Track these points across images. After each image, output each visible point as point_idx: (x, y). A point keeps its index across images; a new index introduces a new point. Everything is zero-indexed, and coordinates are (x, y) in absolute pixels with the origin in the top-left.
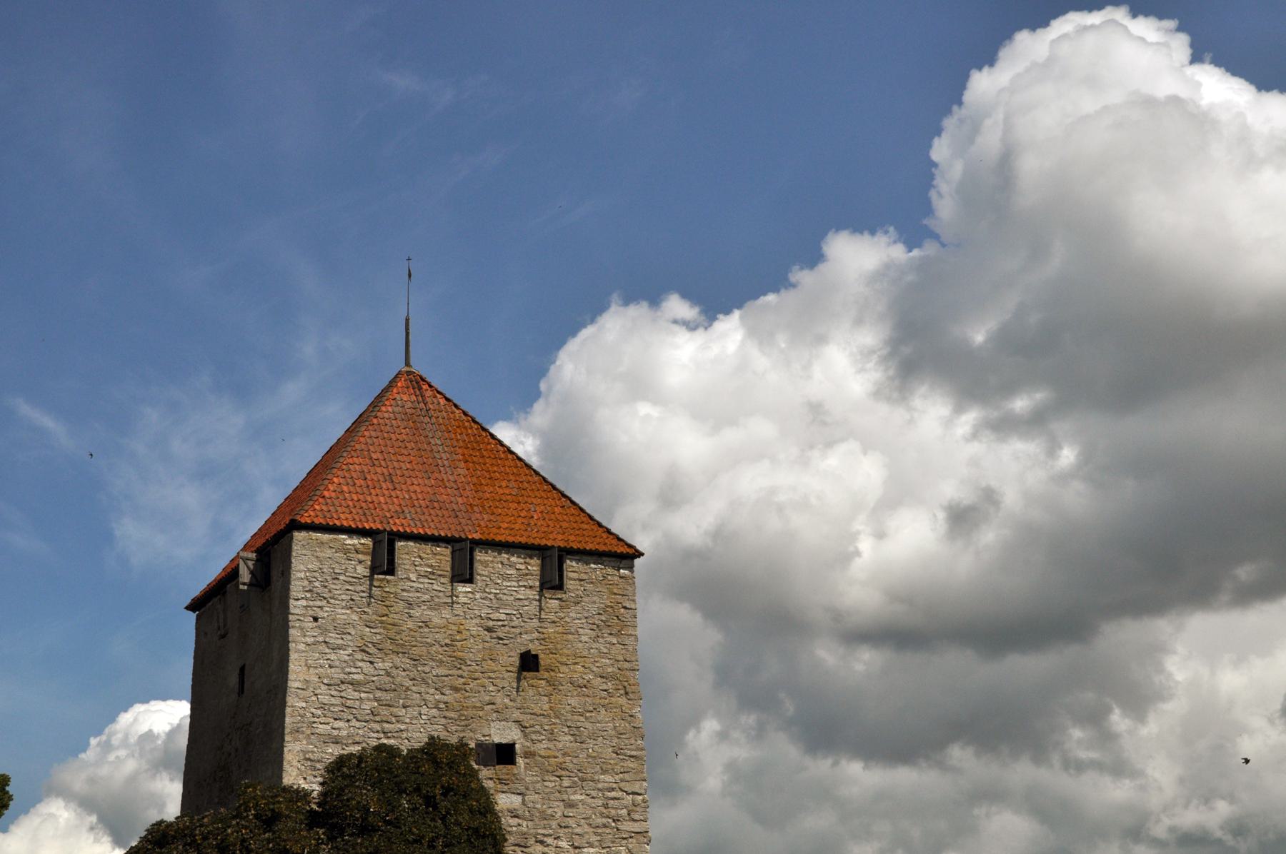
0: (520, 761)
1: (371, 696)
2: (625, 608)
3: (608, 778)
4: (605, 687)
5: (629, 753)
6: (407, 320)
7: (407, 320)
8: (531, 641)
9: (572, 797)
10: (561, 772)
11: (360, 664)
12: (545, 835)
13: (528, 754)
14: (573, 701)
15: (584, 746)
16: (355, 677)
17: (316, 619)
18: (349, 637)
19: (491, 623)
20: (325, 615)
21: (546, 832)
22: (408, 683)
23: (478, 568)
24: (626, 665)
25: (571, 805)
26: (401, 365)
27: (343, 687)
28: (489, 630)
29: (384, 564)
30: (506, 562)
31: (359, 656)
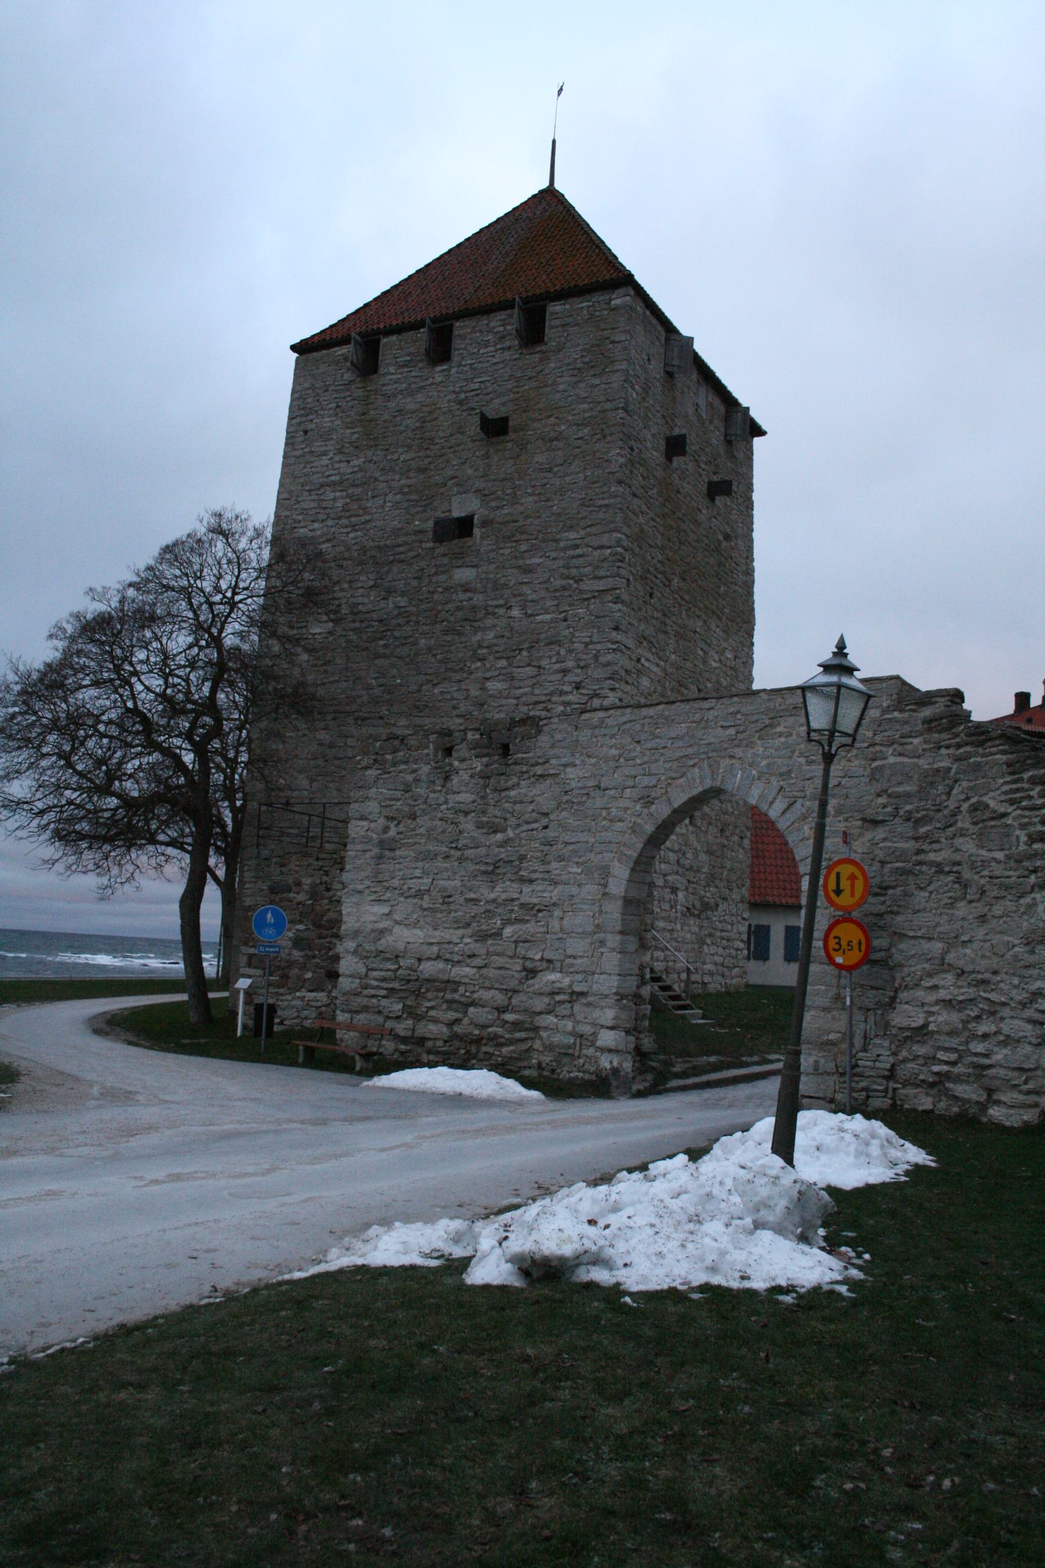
0: (477, 532)
1: (344, 493)
2: (613, 342)
3: (573, 535)
4: (580, 435)
5: (600, 502)
6: (554, 142)
7: (554, 142)
8: (504, 404)
9: (528, 562)
10: (518, 537)
11: (337, 466)
12: (497, 607)
13: (485, 523)
14: (541, 458)
15: (550, 504)
16: (333, 478)
17: (306, 432)
18: (331, 442)
19: (463, 396)
20: (313, 426)
21: (495, 603)
22: (377, 474)
23: (457, 343)
24: (608, 406)
25: (528, 570)
26: (545, 184)
27: (322, 491)
28: (461, 403)
29: (368, 365)
30: (484, 328)
31: (337, 458)
